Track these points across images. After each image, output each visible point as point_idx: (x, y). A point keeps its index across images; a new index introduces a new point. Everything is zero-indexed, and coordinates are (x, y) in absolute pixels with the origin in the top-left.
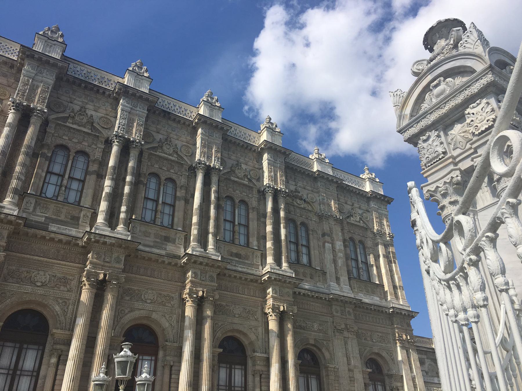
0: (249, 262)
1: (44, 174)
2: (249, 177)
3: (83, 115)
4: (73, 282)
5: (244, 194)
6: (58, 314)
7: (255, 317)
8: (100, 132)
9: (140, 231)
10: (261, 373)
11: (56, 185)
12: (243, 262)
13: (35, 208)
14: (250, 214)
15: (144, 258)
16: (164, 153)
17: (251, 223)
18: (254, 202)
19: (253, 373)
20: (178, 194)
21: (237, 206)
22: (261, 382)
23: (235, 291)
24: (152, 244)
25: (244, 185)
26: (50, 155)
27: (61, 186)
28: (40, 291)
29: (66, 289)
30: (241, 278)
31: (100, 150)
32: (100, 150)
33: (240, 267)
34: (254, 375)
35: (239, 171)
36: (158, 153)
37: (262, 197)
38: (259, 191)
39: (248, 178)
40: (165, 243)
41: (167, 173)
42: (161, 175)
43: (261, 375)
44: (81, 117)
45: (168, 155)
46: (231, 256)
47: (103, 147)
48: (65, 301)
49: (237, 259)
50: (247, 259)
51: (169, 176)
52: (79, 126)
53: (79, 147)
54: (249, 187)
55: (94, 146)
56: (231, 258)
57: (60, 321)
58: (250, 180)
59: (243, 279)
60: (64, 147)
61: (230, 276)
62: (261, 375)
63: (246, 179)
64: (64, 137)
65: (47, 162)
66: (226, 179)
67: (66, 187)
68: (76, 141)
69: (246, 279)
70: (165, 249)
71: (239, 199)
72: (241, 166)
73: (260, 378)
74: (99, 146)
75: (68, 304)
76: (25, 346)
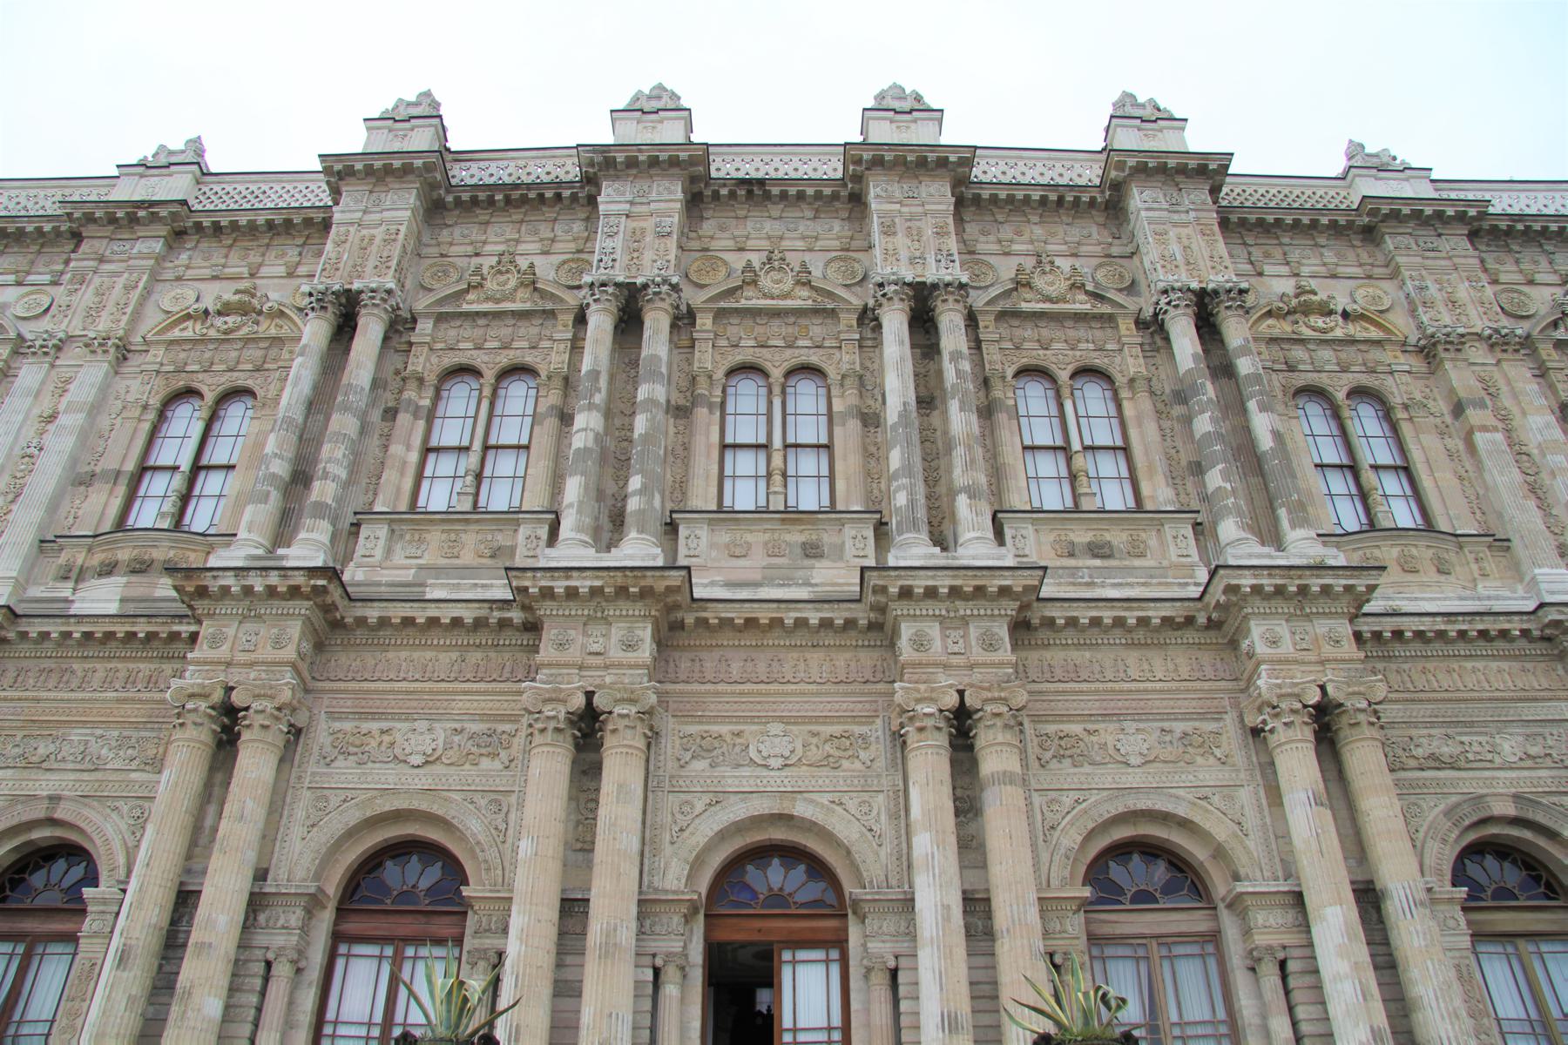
0: (1152, 563)
1: (414, 457)
2: (1090, 287)
3: (507, 272)
4: (516, 741)
5: (1083, 346)
6: (478, 843)
7: (1218, 752)
8: (562, 300)
9: (712, 546)
10: (1281, 955)
11: (734, 477)
12: (1126, 568)
13: (389, 552)
14: (1125, 404)
15: (726, 623)
16: (765, 296)
17: (1133, 433)
18: (1130, 361)
19: (1249, 962)
20: (838, 406)
21: (1066, 392)
22: (1287, 992)
23: (1109, 675)
24: (757, 576)
25: (1079, 317)
26: (426, 402)
27: (769, 476)
28: (422, 779)
29: (497, 765)
30: (1119, 622)
31: (562, 346)
32: (562, 346)
33: (1114, 585)
34: (1253, 969)
35: (1049, 278)
36: (743, 303)
37: (1157, 339)
38: (1141, 324)
39: (1087, 293)
40: (807, 562)
41: (788, 352)
42: (768, 366)
43: (1283, 964)
44: (502, 278)
45: (778, 297)
46: (1071, 555)
47: (569, 335)
48: (496, 801)
49: (1098, 562)
50: (1142, 555)
51: (794, 362)
52: (498, 301)
53: (504, 359)
54: (1100, 317)
55: (545, 344)
56: (1072, 562)
57: (486, 861)
58: (1097, 296)
59: (1132, 621)
60: (466, 371)
61: (1072, 622)
62: (1283, 964)
63: (1082, 297)
64: (461, 346)
65: (421, 424)
66: (1002, 316)
67: (784, 475)
68: (496, 344)
69: (1143, 622)
70: (807, 584)
71: (1071, 368)
72: (1052, 263)
73: (1284, 977)
74: (557, 336)
75: (505, 809)
76: (410, 952)
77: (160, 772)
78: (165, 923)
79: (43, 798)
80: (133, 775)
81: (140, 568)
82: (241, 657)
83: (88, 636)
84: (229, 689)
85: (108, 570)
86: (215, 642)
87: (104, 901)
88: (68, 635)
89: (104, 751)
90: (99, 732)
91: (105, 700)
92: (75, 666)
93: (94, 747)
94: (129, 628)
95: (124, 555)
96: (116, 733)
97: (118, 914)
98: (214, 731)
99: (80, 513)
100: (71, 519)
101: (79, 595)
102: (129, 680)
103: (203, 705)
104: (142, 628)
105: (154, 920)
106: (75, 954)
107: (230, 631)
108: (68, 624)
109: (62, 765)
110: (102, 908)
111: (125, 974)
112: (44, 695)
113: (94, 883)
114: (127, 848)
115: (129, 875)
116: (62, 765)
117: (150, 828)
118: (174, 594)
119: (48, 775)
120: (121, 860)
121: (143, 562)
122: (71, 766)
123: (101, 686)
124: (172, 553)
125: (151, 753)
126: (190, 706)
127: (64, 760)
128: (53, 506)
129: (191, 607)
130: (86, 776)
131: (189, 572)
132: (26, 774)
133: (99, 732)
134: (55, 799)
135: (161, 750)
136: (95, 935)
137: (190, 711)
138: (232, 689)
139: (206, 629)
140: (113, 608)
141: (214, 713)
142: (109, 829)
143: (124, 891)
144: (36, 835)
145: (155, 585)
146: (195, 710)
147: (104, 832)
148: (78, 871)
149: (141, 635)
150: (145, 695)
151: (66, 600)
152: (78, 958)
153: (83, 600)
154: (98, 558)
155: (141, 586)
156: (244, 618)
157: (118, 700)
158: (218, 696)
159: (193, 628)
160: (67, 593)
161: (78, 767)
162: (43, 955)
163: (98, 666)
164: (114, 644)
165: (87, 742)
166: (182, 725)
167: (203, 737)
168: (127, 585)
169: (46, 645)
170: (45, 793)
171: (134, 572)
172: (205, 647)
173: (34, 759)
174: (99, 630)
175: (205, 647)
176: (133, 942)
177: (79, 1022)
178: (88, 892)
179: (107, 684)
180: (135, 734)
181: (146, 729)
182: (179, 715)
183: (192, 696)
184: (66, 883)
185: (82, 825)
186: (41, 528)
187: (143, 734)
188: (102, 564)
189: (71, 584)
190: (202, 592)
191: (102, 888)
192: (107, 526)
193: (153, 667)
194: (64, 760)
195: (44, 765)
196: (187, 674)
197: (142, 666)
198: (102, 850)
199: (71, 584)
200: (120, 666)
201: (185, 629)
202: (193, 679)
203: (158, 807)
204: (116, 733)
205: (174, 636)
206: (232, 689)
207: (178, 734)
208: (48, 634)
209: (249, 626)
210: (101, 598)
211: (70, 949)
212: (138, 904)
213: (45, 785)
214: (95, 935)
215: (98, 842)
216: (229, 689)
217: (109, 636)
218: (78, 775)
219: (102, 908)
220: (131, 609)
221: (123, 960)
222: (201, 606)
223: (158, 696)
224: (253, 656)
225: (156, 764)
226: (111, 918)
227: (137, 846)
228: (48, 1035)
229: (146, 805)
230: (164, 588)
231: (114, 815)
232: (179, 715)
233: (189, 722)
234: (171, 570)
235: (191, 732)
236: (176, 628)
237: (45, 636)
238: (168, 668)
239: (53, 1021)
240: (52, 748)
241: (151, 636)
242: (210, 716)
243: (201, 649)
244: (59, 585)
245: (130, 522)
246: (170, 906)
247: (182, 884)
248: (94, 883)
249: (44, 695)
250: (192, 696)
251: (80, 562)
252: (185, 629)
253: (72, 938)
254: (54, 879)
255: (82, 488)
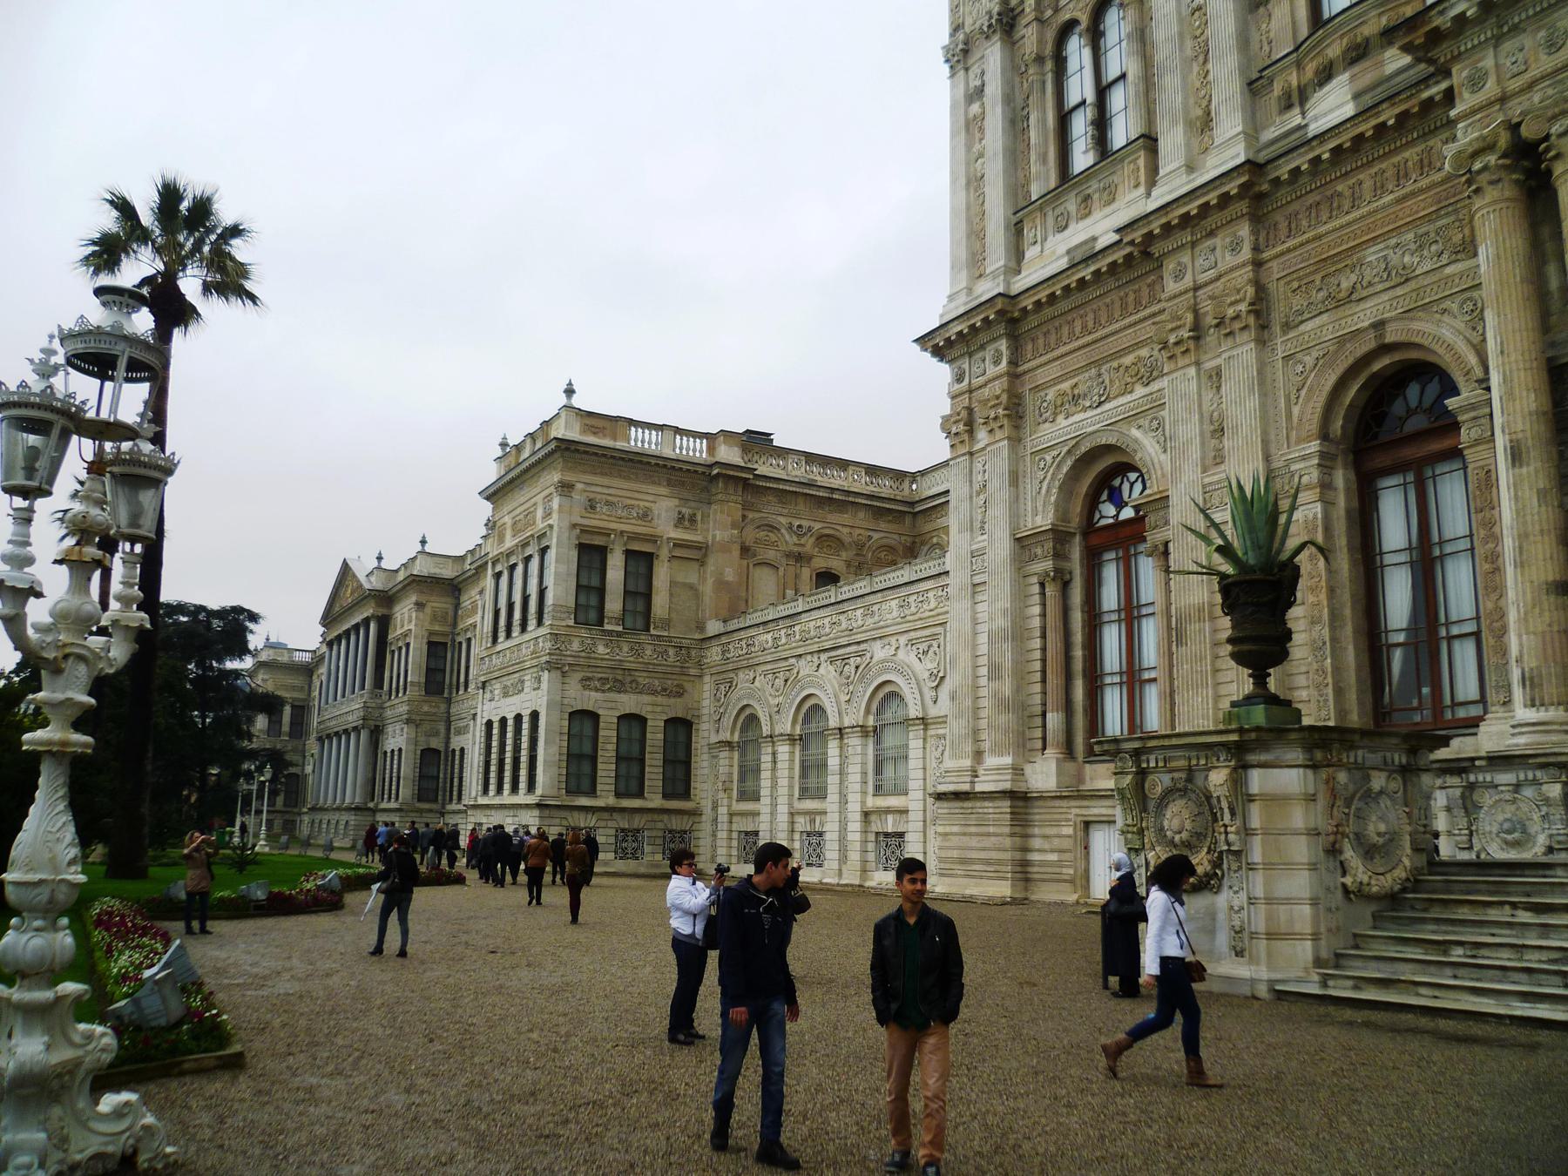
77: (1475, 255)
78: (1546, 403)
79: (1366, 329)
80: (1448, 270)
81: (1358, 53)
82: (1514, 85)
83: (1337, 151)
84: (1514, 128)
85: (1326, 75)
86: (1476, 83)
87: (1473, 407)
88: (1316, 161)
89: (1407, 259)
90: (1393, 241)
91: (1384, 207)
92: (1340, 188)
93: (1395, 259)
94: (1374, 122)
95: (1334, 50)
96: (1410, 236)
97: (1491, 415)
98: (1517, 182)
99: (1272, 35)
100: (1266, 48)
101: (1310, 115)
102: (1401, 175)
103: (1492, 159)
104: (1388, 116)
105: (1533, 406)
106: (1465, 468)
107: (1488, 62)
108: (1312, 149)
109: (1371, 290)
110: (1473, 414)
111: (1524, 470)
112: (1323, 229)
113: (1455, 392)
114: (1474, 346)
115: (1486, 370)
116: (1371, 290)
117: (1489, 315)
118: (1408, 59)
119: (1363, 305)
120: (1473, 360)
121: (1358, 46)
122: (1380, 287)
123: (1374, 196)
124: (1384, 21)
125: (1457, 238)
126: (1477, 166)
127: (1370, 284)
128: (1244, 42)
129: (1431, 61)
130: (1399, 291)
131: (1411, 23)
132: (1340, 313)
133: (1393, 241)
134: (1379, 325)
135: (1467, 231)
136: (1477, 442)
137: (1479, 172)
138: (1519, 124)
139: (1460, 74)
140: (1349, 110)
141: (1507, 162)
142: (1447, 334)
143: (1488, 389)
144: (1377, 366)
145: (1382, 64)
146: (1485, 168)
147: (1443, 336)
148: (1433, 389)
149: (1391, 122)
150: (1423, 183)
151: (1299, 128)
152: (1471, 467)
153: (1316, 118)
154: (1310, 69)
155: (1367, 73)
156: (1498, 40)
157: (1399, 201)
158: (1504, 140)
159: (1444, 85)
160: (1298, 120)
161: (1387, 285)
162: (1434, 477)
163: (1361, 177)
164: (1367, 146)
165: (1385, 257)
166: (1477, 191)
167: (1507, 194)
168: (1353, 78)
169: (1304, 179)
170: (1366, 324)
171: (1354, 61)
172: (1466, 95)
173: (1343, 295)
174: (1345, 139)
175: (1466, 95)
176: (1520, 436)
177: (1496, 529)
178: (1452, 403)
179: (1379, 189)
180: (1431, 227)
181: (1441, 217)
182: (1469, 182)
183: (1475, 155)
184: (1427, 402)
185: (1418, 340)
186: (1243, 69)
187: (1440, 223)
188: (1317, 73)
189: (1297, 110)
190: (1436, 36)
191: (1464, 395)
192: (1304, 31)
193: (1418, 149)
194: (1370, 284)
195: (1353, 297)
196: (1459, 134)
197: (1407, 154)
198: (1448, 358)
199: (1297, 110)
200: (1383, 166)
201: (1435, 90)
202: (1466, 136)
203: (1488, 292)
204: (1410, 236)
205: (1428, 104)
206: (1519, 124)
207: (1478, 202)
208: (1298, 168)
209: (1507, 46)
210: (1333, 105)
211: (1457, 465)
212: (1509, 395)
213: (1363, 316)
214: (1477, 442)
215: (1441, 351)
216: (1514, 128)
217: (1359, 139)
218: (1391, 294)
219: (1473, 414)
220: (1368, 100)
221: (1516, 456)
222: (1442, 53)
223: (1437, 177)
224: (1527, 77)
225: (1468, 248)
226: (1485, 421)
227: (1484, 340)
228: (1472, 549)
229: (1475, 294)
230: (1395, 60)
231: (1446, 318)
232: (1469, 182)
233: (1484, 184)
234: (1388, 35)
235: (1491, 194)
236: (1425, 95)
237: (1296, 172)
238: (1435, 142)
239: (1471, 536)
240: (1353, 278)
241: (1403, 118)
242: (1504, 167)
243: (1463, 100)
244: (1287, 116)
245: (1326, 15)
246: (1545, 387)
247: (1550, 360)
248: (1455, 392)
249: (1323, 229)
250: (1475, 155)
251: (1295, 83)
252: (1435, 90)
253: (1455, 454)
254: (1413, 403)
255: (1262, 9)
